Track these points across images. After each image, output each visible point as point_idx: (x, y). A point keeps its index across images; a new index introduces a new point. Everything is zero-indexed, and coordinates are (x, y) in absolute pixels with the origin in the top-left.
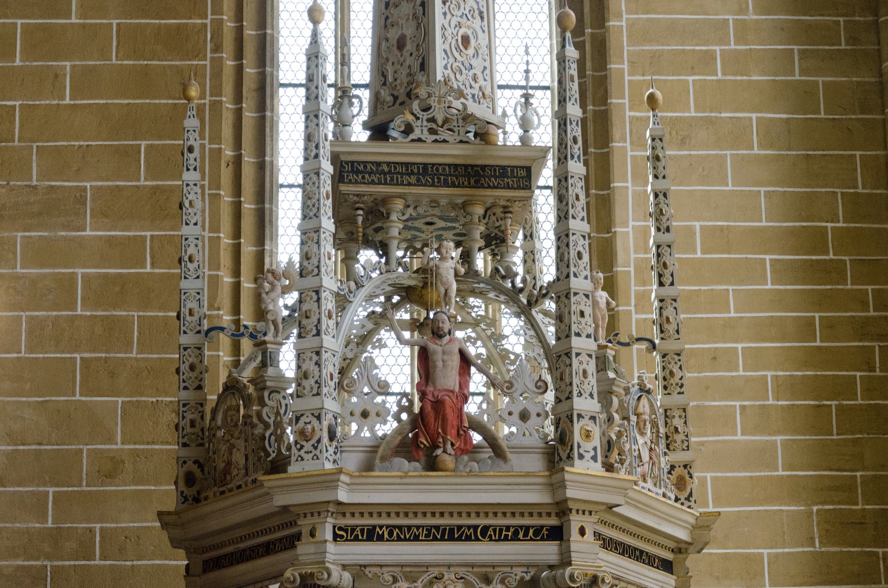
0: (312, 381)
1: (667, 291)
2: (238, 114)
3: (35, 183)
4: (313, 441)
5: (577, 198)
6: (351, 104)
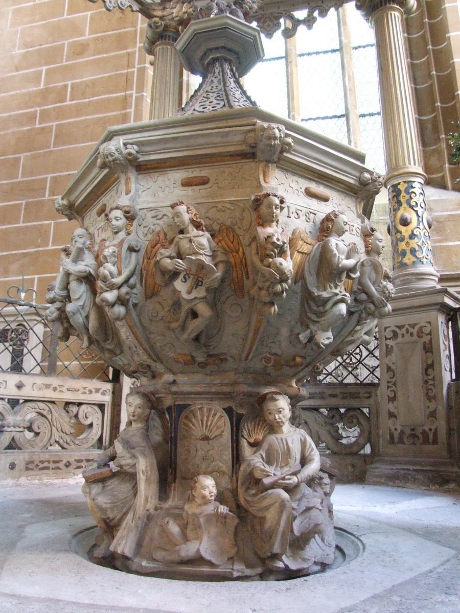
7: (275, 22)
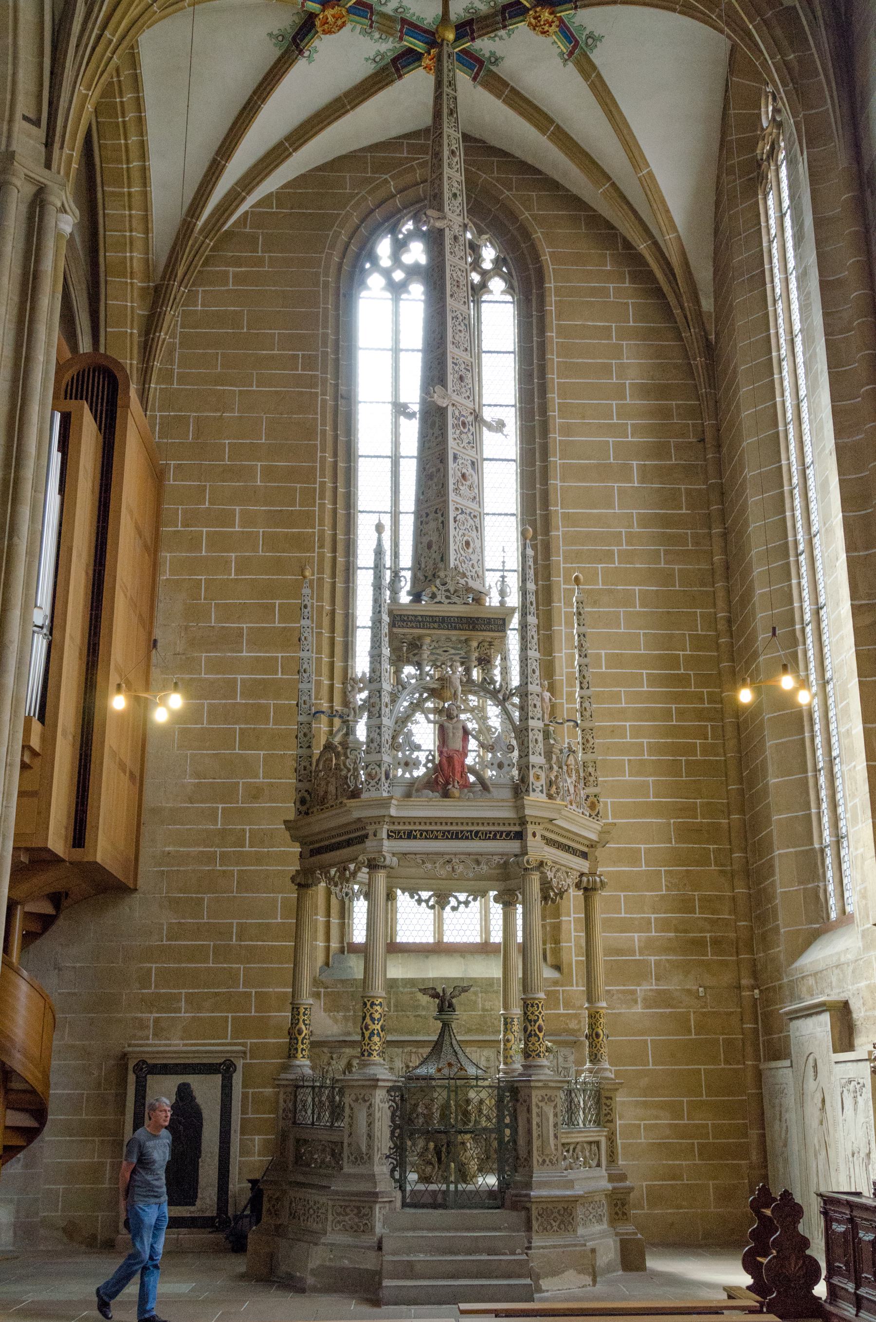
0: (376, 744)
1: (586, 692)
2: (334, 585)
3: (213, 624)
4: (376, 780)
5: (533, 637)
6: (400, 581)
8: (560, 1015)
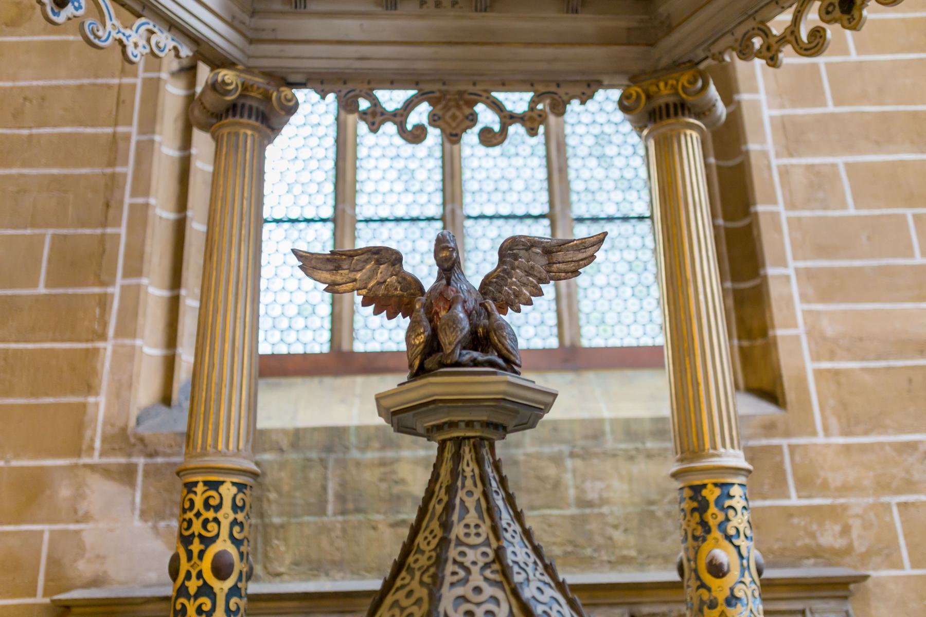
7: (467, 111)
8: (789, 513)
